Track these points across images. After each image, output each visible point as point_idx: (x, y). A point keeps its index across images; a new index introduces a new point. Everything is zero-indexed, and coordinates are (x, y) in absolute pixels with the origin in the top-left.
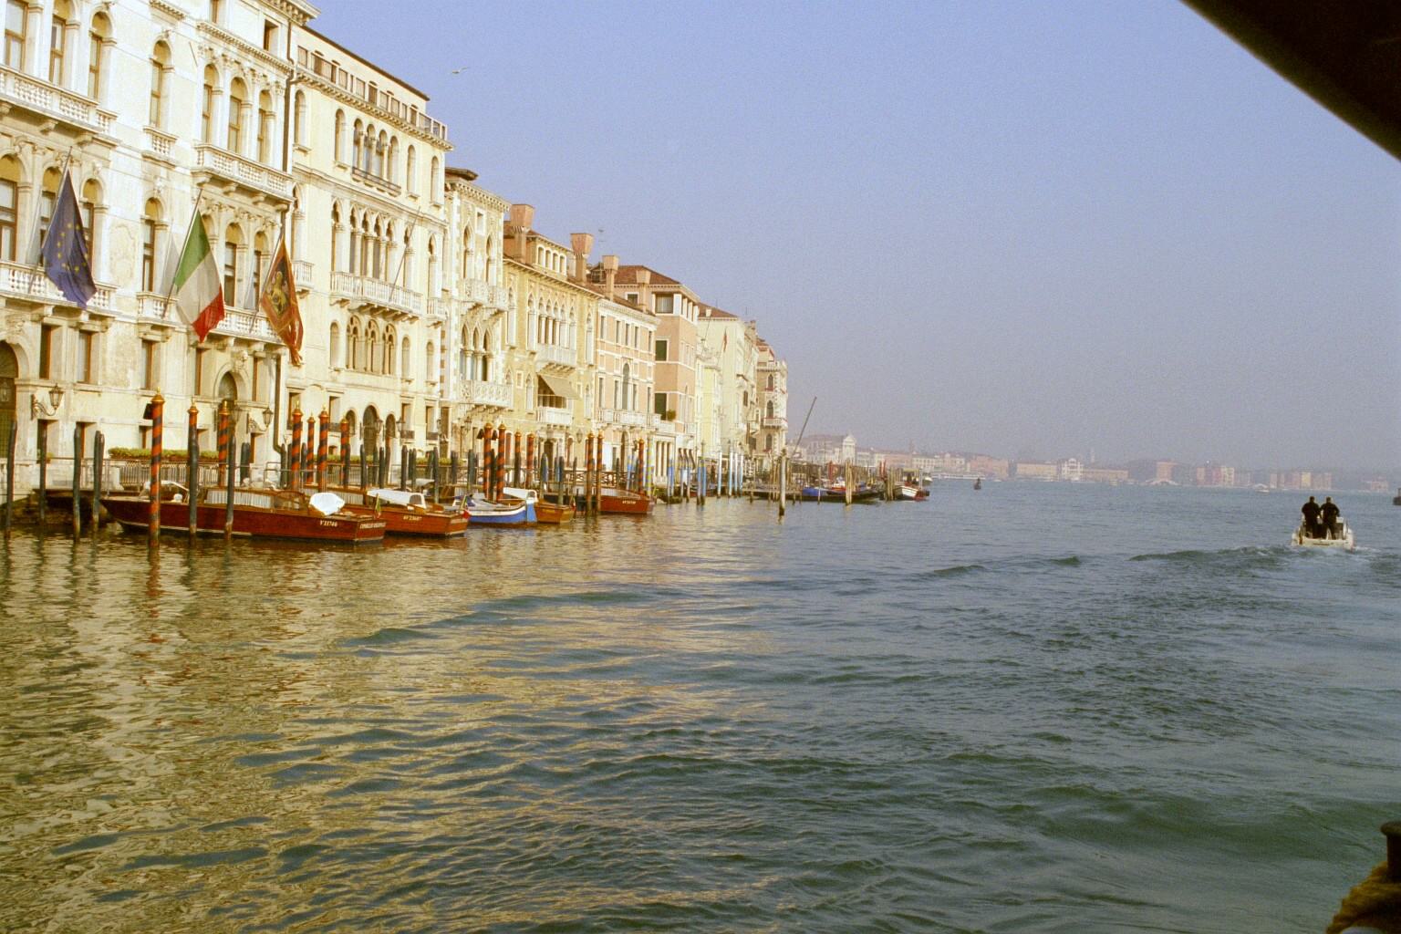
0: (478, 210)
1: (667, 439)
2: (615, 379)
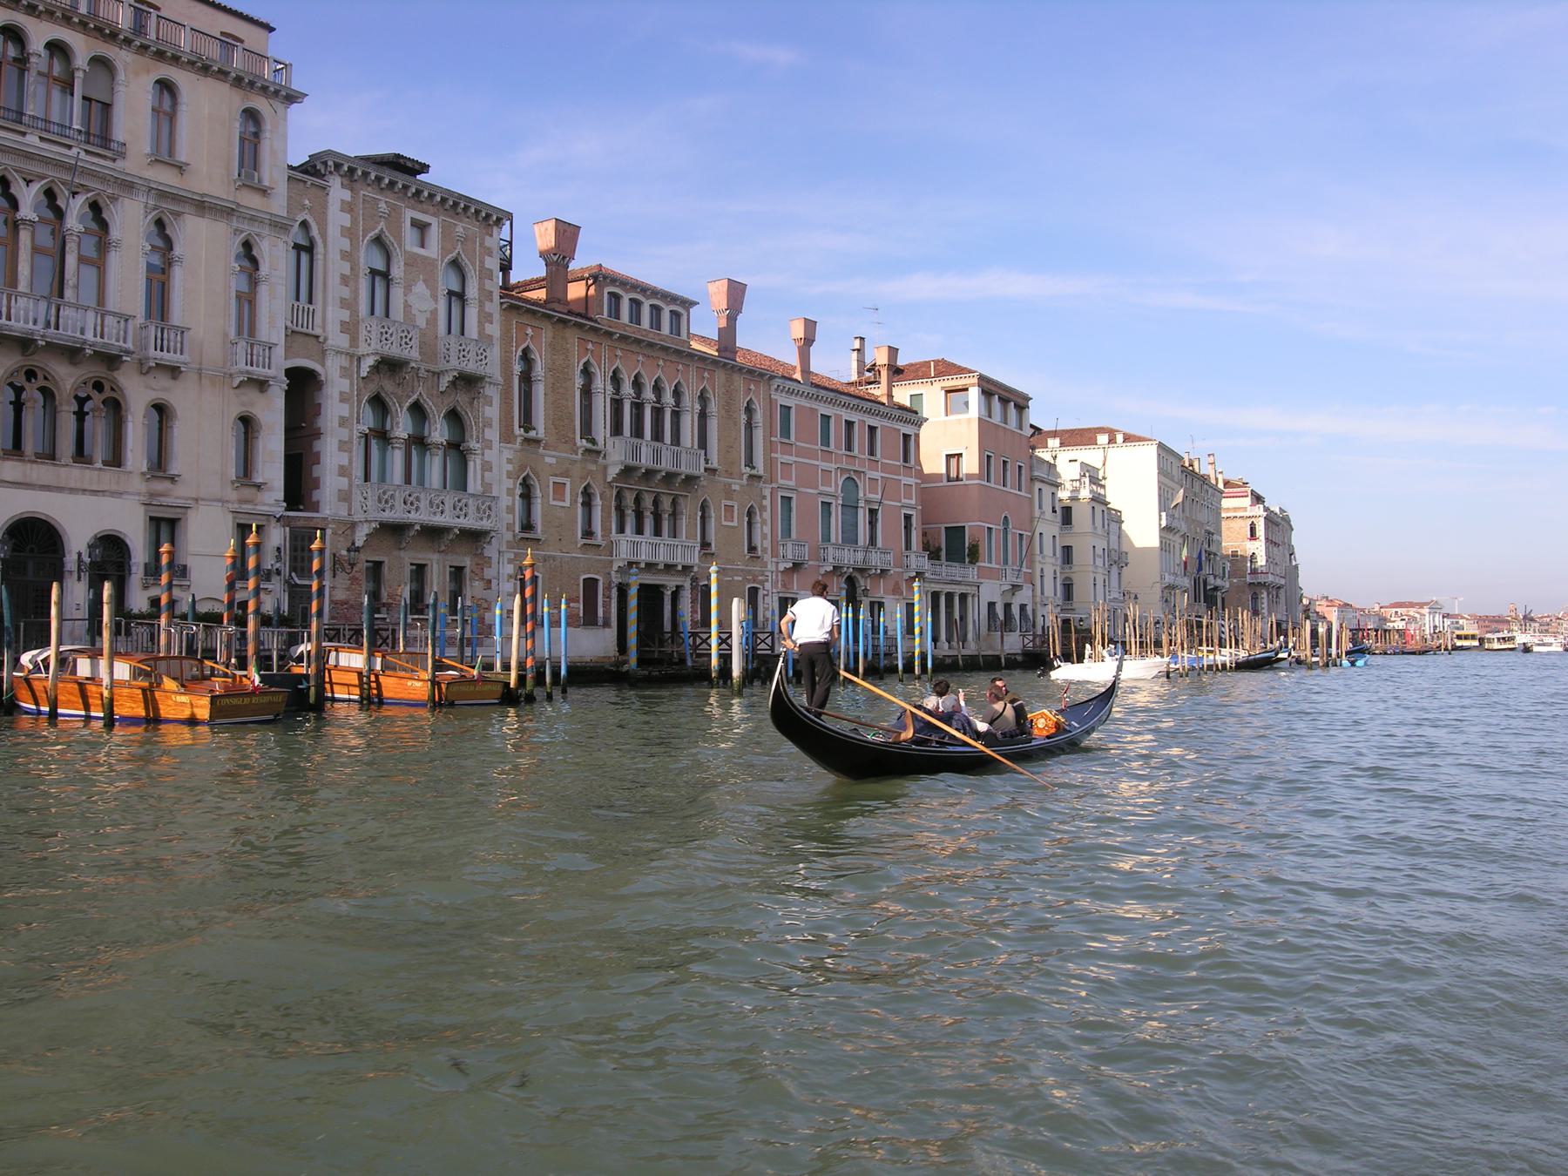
0: (409, 214)
1: (958, 590)
2: (904, 511)
